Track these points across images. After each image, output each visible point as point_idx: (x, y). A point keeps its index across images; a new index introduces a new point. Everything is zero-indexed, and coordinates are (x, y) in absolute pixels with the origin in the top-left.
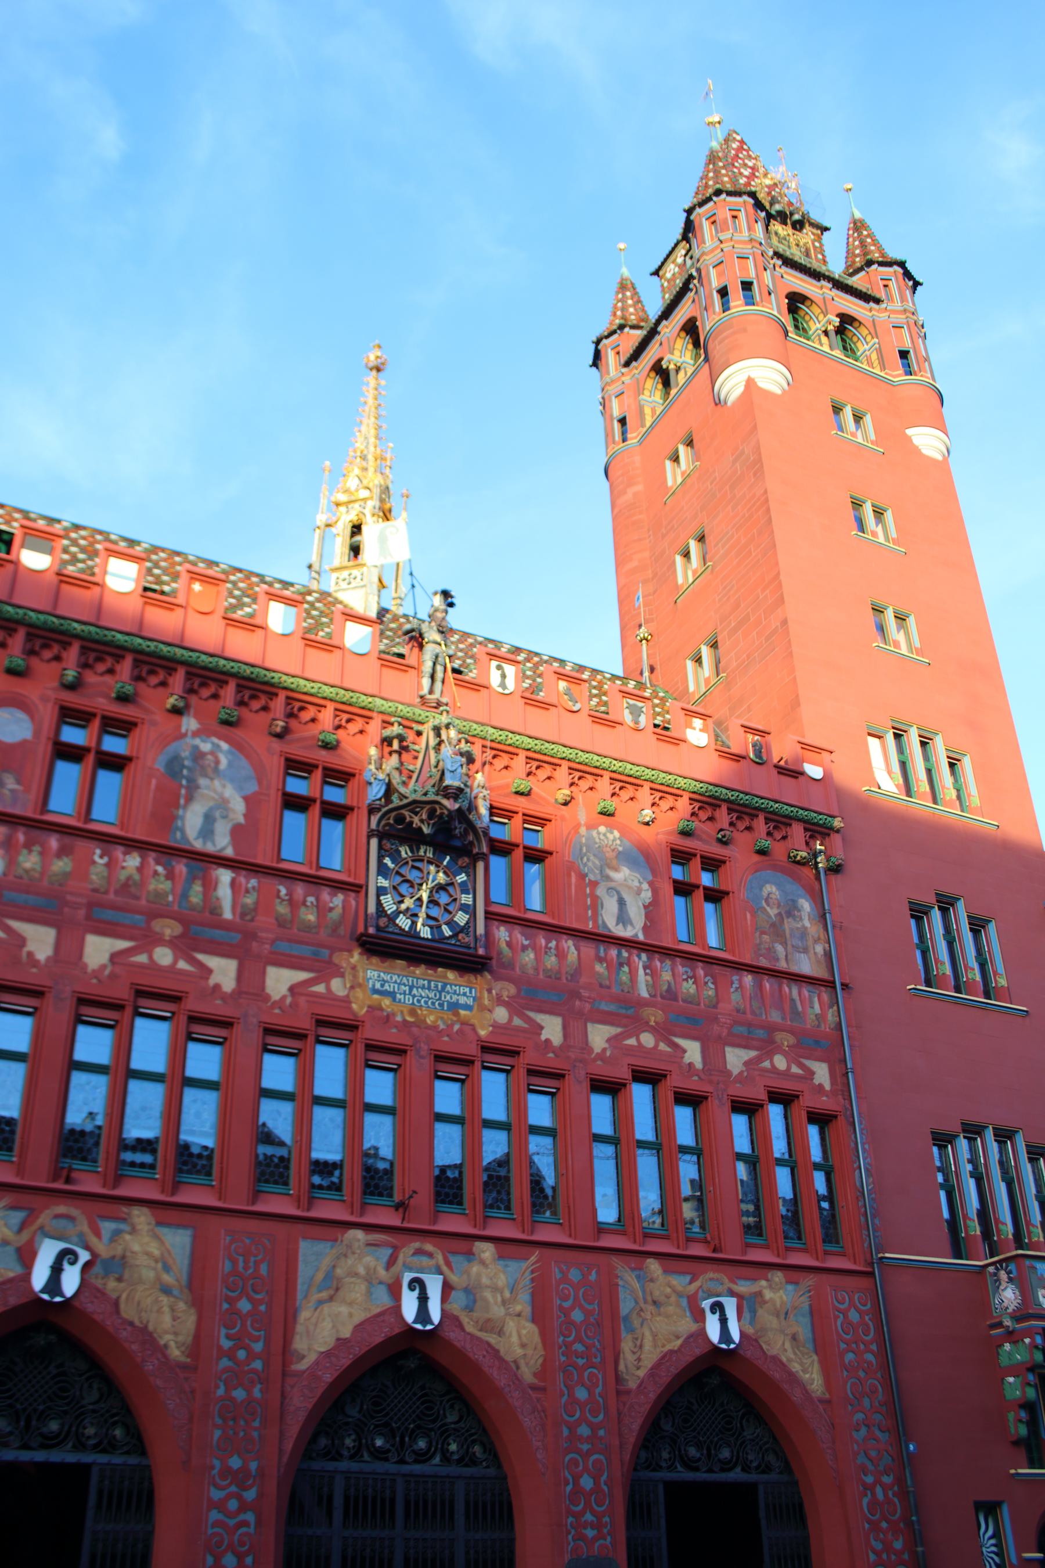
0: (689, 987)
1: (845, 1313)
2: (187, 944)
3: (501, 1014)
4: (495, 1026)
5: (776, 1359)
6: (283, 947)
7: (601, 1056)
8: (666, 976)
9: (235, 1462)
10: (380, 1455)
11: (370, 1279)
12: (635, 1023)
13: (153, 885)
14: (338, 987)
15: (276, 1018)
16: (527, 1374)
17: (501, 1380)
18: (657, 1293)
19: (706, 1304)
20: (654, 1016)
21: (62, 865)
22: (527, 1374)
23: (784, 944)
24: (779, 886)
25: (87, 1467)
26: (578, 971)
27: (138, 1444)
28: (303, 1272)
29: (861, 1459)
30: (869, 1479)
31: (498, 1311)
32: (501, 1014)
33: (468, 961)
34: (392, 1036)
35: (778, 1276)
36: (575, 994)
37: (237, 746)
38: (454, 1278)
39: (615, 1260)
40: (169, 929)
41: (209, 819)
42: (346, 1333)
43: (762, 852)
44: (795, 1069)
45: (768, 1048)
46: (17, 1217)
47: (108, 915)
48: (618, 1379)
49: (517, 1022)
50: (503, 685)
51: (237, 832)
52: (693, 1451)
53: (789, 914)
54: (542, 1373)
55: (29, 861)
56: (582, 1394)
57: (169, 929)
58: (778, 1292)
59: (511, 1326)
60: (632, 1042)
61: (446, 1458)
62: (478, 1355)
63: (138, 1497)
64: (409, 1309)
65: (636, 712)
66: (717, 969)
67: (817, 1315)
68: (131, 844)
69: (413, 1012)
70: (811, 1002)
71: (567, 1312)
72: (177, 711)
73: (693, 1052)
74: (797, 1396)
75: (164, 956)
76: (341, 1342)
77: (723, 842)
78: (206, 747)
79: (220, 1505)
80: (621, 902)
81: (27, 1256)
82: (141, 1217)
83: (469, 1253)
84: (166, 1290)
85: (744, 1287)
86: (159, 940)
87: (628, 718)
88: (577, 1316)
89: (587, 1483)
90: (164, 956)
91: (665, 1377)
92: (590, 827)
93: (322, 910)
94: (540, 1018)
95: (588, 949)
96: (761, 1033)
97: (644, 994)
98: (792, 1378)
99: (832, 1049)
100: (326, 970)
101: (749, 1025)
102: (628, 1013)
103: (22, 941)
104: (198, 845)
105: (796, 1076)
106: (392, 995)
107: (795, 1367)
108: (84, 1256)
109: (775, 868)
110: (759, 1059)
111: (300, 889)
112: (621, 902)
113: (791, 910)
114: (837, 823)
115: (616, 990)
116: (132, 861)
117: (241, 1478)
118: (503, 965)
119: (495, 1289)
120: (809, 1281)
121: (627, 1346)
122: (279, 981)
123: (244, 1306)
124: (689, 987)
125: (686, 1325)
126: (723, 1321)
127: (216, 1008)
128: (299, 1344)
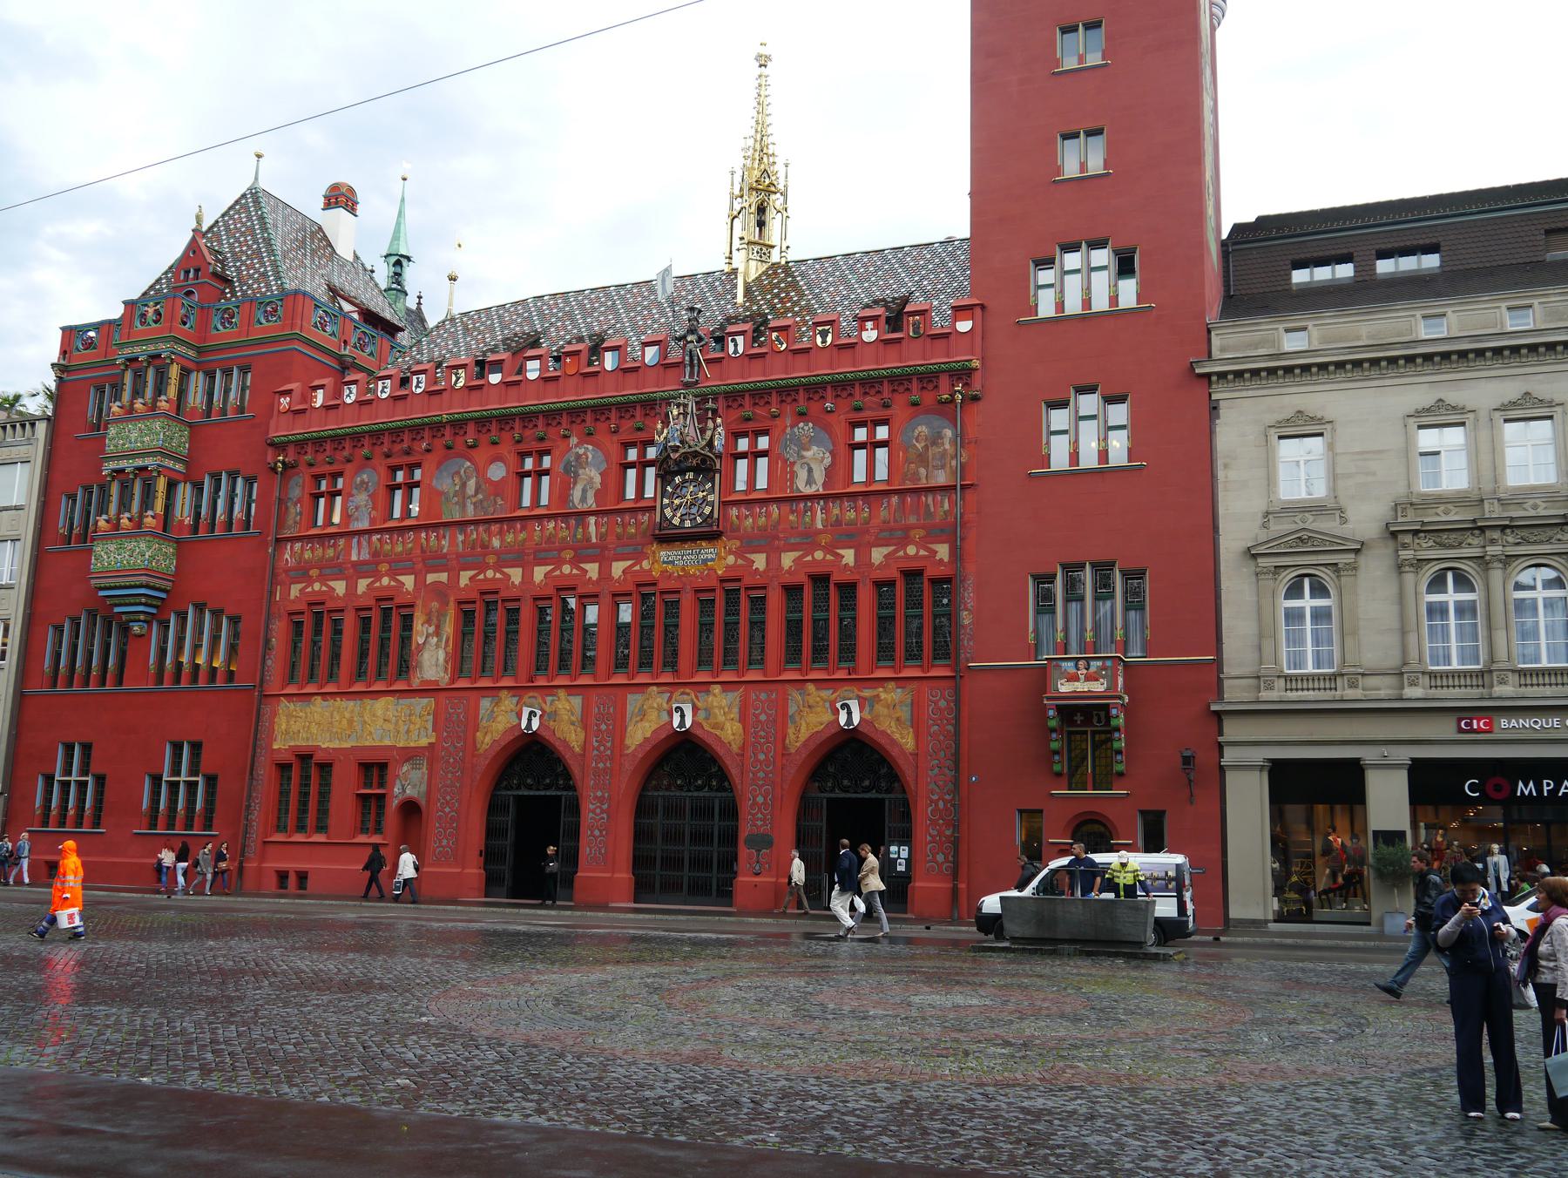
0: (852, 515)
1: (936, 703)
2: (576, 562)
3: (731, 559)
4: (727, 567)
5: (884, 733)
6: (620, 550)
7: (789, 572)
8: (836, 511)
9: (599, 794)
10: (680, 788)
11: (659, 709)
12: (813, 546)
13: (561, 534)
14: (646, 565)
15: (618, 588)
16: (735, 748)
17: (721, 752)
18: (811, 702)
19: (838, 705)
20: (824, 539)
21: (522, 536)
22: (735, 748)
23: (927, 467)
24: (927, 425)
25: (559, 797)
26: (779, 522)
27: (574, 788)
28: (630, 709)
29: (932, 786)
30: (935, 797)
31: (721, 719)
32: (731, 559)
33: (709, 534)
34: (673, 585)
35: (891, 685)
36: (776, 537)
37: (596, 445)
38: (699, 704)
39: (788, 686)
40: (568, 555)
41: (584, 491)
42: (648, 735)
43: (915, 404)
44: (922, 553)
45: (904, 542)
46: (515, 700)
47: (543, 555)
48: (784, 747)
49: (740, 562)
50: (736, 351)
51: (597, 494)
52: (846, 782)
53: (934, 443)
54: (743, 748)
55: (509, 538)
56: (762, 757)
57: (568, 555)
58: (891, 695)
59: (728, 725)
60: (809, 558)
61: (711, 789)
62: (710, 741)
63: (575, 808)
64: (676, 723)
65: (824, 334)
66: (872, 498)
67: (916, 706)
68: (549, 517)
69: (683, 569)
70: (942, 502)
71: (757, 716)
72: (566, 437)
73: (849, 556)
74: (895, 752)
75: (566, 569)
76: (646, 740)
77: (886, 406)
78: (581, 451)
79: (593, 811)
80: (810, 471)
81: (519, 716)
82: (562, 693)
83: (708, 692)
84: (573, 723)
85: (867, 693)
86: (565, 562)
87: (819, 339)
88: (763, 717)
89: (760, 799)
90: (566, 569)
91: (812, 746)
92: (792, 427)
93: (638, 524)
94: (752, 556)
95: (786, 507)
96: (899, 533)
97: (820, 526)
98: (893, 742)
99: (950, 532)
100: (639, 557)
101: (892, 530)
102: (809, 540)
103: (508, 577)
104: (580, 507)
105: (924, 557)
106: (672, 562)
107: (897, 736)
108: (539, 713)
109: (927, 412)
110: (895, 551)
111: (627, 517)
112: (810, 471)
113: (936, 439)
114: (976, 364)
115: (802, 528)
116: (552, 525)
117: (601, 800)
118: (733, 531)
119: (720, 707)
120: (914, 685)
121: (791, 731)
122: (618, 568)
123: (603, 727)
124: (852, 515)
125: (828, 717)
126: (850, 713)
127: (590, 589)
128: (628, 742)
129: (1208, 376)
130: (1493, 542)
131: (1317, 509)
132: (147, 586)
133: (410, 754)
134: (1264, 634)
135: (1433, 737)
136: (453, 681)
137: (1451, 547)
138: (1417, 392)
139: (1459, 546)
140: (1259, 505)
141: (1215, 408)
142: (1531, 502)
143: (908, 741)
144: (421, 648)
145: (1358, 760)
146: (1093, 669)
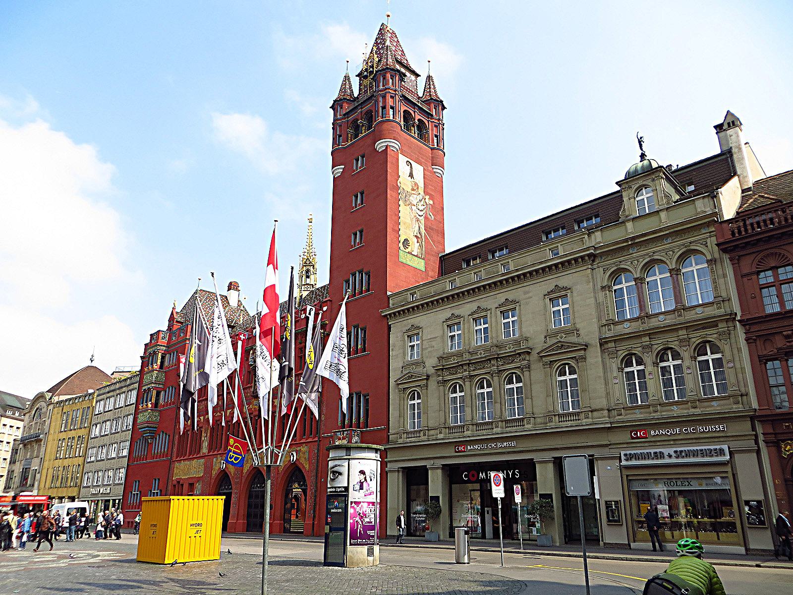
35: (304, 445)
58: (304, 449)
85: (298, 449)
98: (304, 467)
126: (293, 457)
129: (386, 316)
130: (465, 371)
131: (416, 364)
132: (148, 427)
133: (198, 479)
134: (402, 415)
135: (446, 455)
136: (209, 453)
137: (454, 374)
138: (444, 313)
139: (456, 373)
140: (401, 365)
141: (389, 328)
142: (479, 352)
143: (307, 466)
144: (203, 441)
145: (533, 459)
146: (345, 435)
